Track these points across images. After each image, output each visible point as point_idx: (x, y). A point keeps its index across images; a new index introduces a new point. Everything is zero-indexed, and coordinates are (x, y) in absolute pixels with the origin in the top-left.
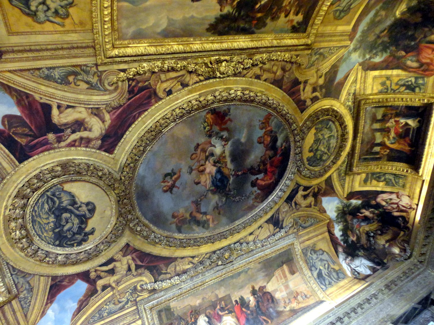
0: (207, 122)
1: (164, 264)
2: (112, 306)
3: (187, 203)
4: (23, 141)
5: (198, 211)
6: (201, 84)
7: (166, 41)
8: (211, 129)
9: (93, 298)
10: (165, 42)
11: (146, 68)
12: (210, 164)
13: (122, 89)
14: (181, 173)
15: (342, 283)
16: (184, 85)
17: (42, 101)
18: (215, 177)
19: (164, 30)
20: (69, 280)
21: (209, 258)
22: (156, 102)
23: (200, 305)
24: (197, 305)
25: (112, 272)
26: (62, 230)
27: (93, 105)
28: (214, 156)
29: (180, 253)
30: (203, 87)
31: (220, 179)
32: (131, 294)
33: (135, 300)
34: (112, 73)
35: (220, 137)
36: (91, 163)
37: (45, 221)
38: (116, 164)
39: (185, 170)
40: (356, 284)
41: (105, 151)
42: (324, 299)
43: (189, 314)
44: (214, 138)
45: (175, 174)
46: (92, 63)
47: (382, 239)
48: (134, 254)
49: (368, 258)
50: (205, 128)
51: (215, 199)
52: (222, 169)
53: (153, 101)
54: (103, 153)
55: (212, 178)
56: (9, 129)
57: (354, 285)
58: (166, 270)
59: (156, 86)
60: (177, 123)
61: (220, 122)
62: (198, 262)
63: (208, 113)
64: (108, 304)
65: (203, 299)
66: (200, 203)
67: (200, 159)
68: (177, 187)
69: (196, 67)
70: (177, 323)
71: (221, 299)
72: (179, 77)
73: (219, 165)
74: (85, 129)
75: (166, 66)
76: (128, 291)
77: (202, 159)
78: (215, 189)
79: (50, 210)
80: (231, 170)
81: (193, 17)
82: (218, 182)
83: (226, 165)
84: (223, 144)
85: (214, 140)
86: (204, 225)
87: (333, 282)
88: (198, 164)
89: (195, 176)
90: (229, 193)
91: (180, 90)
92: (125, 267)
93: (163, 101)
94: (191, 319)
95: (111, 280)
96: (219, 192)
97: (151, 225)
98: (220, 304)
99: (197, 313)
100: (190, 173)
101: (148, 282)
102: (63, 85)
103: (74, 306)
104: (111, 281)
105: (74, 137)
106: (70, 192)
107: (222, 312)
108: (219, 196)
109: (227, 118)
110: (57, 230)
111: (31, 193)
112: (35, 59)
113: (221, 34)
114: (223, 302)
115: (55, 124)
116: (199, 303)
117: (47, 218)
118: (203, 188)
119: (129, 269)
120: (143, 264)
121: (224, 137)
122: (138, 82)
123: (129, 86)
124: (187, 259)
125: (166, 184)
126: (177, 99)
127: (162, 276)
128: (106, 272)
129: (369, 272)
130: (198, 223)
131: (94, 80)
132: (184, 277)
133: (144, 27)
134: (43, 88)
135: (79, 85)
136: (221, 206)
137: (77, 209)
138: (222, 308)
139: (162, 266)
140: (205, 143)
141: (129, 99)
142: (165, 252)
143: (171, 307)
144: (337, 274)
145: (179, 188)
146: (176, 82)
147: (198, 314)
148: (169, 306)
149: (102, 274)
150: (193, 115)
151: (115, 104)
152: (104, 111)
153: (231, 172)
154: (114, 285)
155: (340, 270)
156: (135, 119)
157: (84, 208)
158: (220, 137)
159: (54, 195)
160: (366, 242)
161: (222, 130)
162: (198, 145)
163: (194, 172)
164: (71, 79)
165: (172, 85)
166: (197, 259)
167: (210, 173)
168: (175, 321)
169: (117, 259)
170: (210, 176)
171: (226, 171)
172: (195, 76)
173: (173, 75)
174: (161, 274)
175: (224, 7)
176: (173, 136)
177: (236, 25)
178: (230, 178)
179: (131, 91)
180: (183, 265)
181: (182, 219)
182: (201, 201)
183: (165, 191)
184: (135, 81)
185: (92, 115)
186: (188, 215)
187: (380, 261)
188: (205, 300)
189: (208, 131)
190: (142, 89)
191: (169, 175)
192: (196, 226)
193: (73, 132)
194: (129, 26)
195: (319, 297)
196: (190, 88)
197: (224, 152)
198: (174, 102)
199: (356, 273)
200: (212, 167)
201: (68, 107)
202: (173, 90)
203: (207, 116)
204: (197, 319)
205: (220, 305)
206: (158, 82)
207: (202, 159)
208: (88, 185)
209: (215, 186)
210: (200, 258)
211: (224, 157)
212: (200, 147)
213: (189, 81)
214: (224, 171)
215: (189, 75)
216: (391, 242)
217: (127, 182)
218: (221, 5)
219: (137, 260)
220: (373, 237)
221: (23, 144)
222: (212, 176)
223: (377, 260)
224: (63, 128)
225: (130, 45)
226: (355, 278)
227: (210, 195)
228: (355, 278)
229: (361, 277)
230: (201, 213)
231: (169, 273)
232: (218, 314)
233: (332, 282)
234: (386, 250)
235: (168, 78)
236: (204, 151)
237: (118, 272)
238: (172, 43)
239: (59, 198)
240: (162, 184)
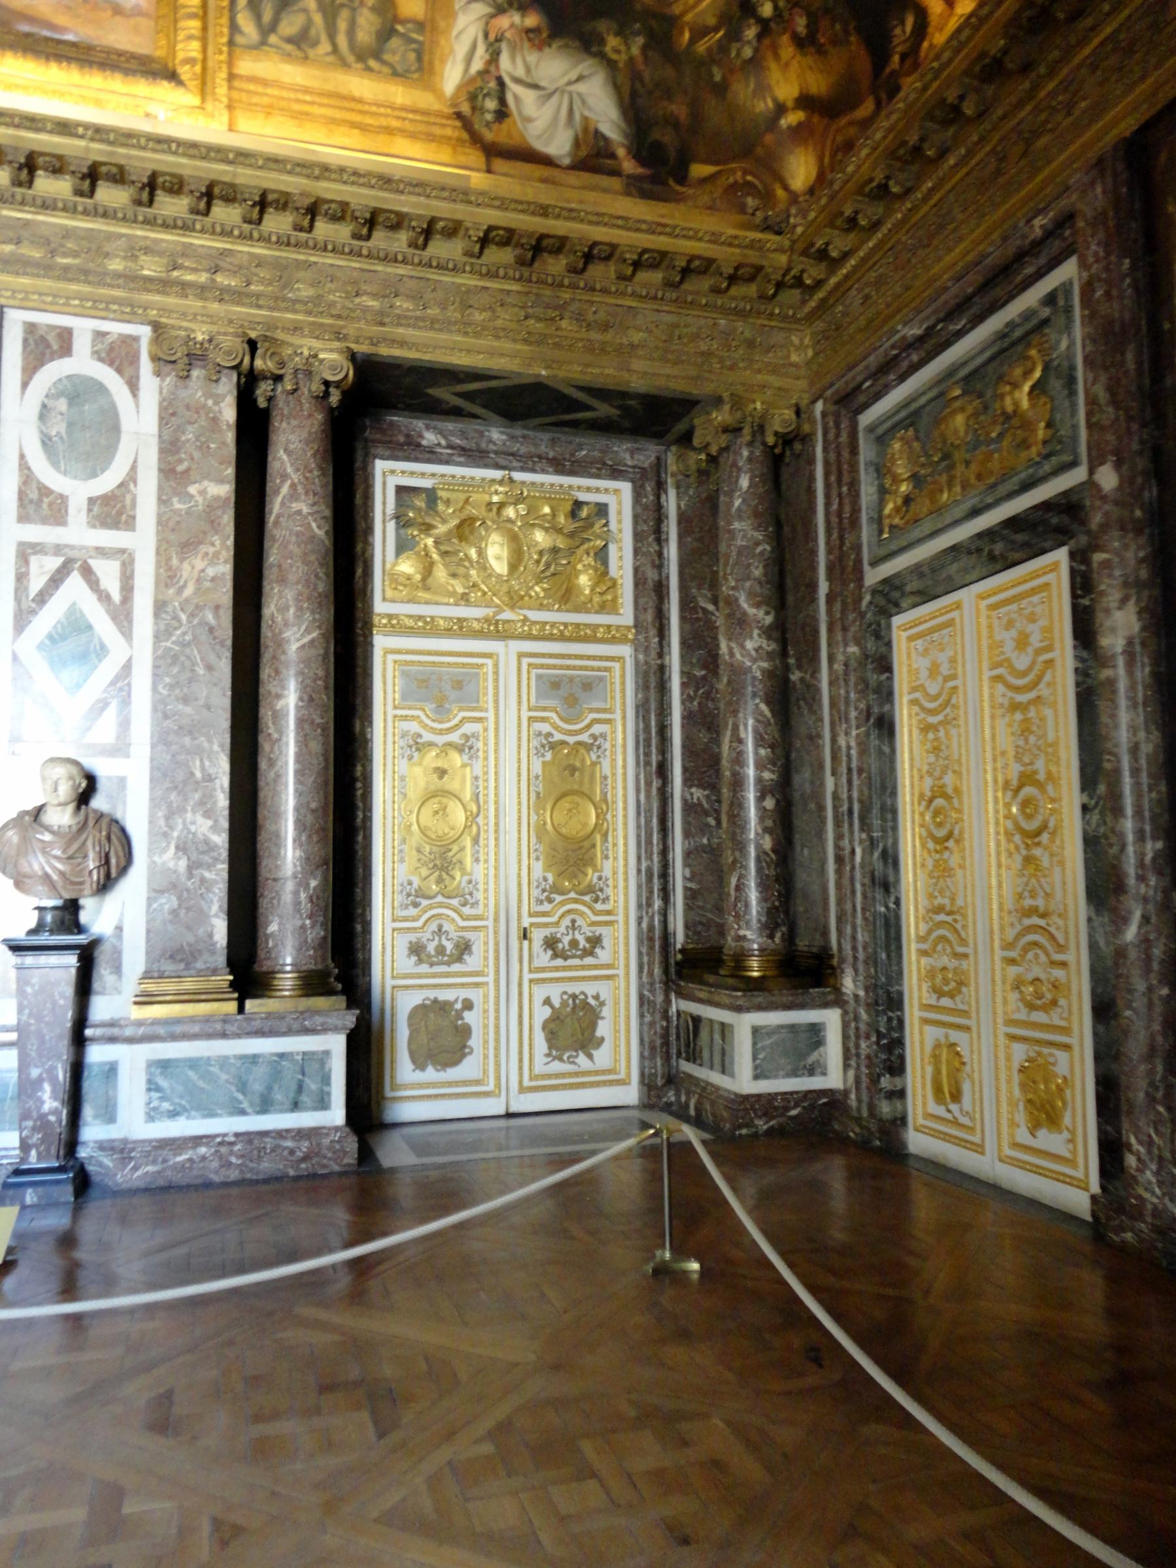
15: (361, 85)
40: (431, 138)
42: (184, 72)
47: (793, 72)
49: (634, 94)
57: (413, 136)
87: (325, 47)
129: (559, 146)
144: (386, 33)
155: (420, 26)
160: (712, 21)
187: (672, 154)
195: (173, 52)
199: (491, 104)
216: (816, 119)
220: (765, 28)
223: (666, 137)
226: (459, 116)
228: (459, 116)
229: (489, 136)
233: (315, 43)
234: (769, 138)
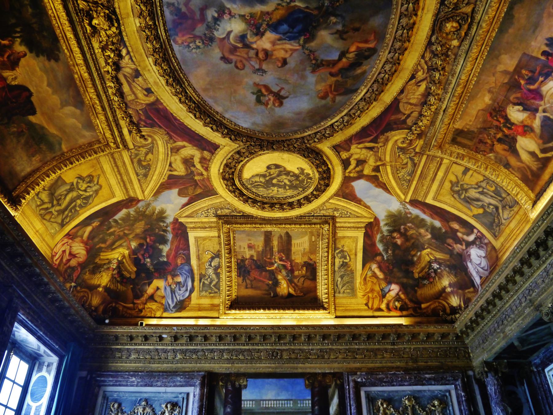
0: (189, 43)
1: (392, 115)
2: (404, 171)
3: (312, 79)
4: (199, 191)
5: (334, 63)
6: (132, 54)
7: (87, 102)
8: (200, 37)
9: (380, 179)
10: (89, 103)
11: (123, 115)
12: (258, 42)
13: (150, 132)
14: (262, 83)
16: (137, 74)
17: (166, 178)
18: (284, 34)
19: (76, 106)
20: (346, 188)
21: (435, 55)
22: (162, 104)
23: (494, 100)
24: (490, 102)
25: (361, 162)
26: (288, 185)
27: (168, 151)
28: (247, 34)
29: (388, 97)
30: (137, 52)
31: (289, 26)
32: (404, 153)
33: (416, 153)
34: (133, 139)
35: (215, 23)
36: (225, 162)
37: (275, 192)
38: (230, 145)
39: (257, 78)
41: (216, 150)
43: (490, 119)
44: (215, 33)
45: (260, 91)
46: (127, 152)
48: (353, 141)
50: (198, 47)
51: (325, 37)
52: (274, 20)
53: (160, 107)
54: (216, 152)
55: (285, 39)
56: (189, 195)
58: (405, 114)
59: (143, 104)
60: (189, 84)
61: (190, 22)
62: (428, 72)
63: (176, 42)
64: (398, 172)
65: (489, 91)
66: (319, 62)
67: (246, 56)
68: (280, 91)
69: (111, 64)
70: (485, 135)
71: (518, 70)
72: (128, 81)
73: (264, 26)
74: (193, 159)
75: (116, 99)
76: (399, 155)
77: (247, 54)
78: (305, 35)
79: (265, 188)
80: (279, 4)
81: (49, 85)
82: (295, 30)
83: (268, 13)
84: (229, 16)
85: (219, 34)
86: (365, 56)
88: (254, 60)
89: (271, 66)
90: (325, 8)
91: (145, 80)
92: (364, 151)
93: (159, 97)
94: (498, 120)
95: (372, 162)
96: (315, 28)
97: (322, 124)
98: (521, 76)
99: (499, 111)
100: (264, 72)
101: (404, 136)
102: (151, 168)
103: (379, 191)
104: (374, 164)
105: (198, 166)
106: (253, 176)
107: (534, 85)
108: (321, 29)
109: (184, 9)
110: (287, 188)
111: (244, 197)
112: (131, 182)
113: (55, 40)
114: (524, 72)
115: (186, 175)
116: (490, 100)
117: (273, 191)
118: (295, 55)
119: (371, 149)
120: (375, 135)
121: (216, 15)
122: (140, 119)
123: (145, 126)
124: (409, 87)
125: (271, 103)
126: (155, 83)
127: (409, 122)
128: (357, 165)
130: (356, 64)
131: (143, 150)
132: (432, 100)
133: (80, 125)
134: (154, 178)
135: (150, 159)
136: (344, 26)
137: (270, 175)
138: (529, 79)
139: (393, 117)
140: (222, 49)
141: (160, 127)
142: (375, 111)
143: (460, 128)
145: (282, 88)
146: (134, 84)
147: (501, 111)
148: (457, 130)
149: (357, 169)
150: (177, 65)
151: (166, 137)
152: (174, 145)
153: (284, 4)
154: (379, 163)
156: (182, 124)
157: (272, 171)
158: (215, 23)
159: (251, 184)
161: (203, 18)
162: (224, 59)
163: (264, 67)
164: (144, 163)
165: (139, 88)
166: (420, 73)
167: (274, 43)
168: (481, 136)
169: (348, 157)
170: (279, 42)
171: (277, 16)
172: (123, 60)
173: (126, 88)
174: (404, 122)
175: (19, 53)
176: (205, 90)
177: (34, 20)
178: (296, 6)
179: (152, 126)
180: (415, 93)
181: (335, 86)
182: (317, 60)
183: (281, 104)
184: (140, 122)
185: (178, 153)
186: (334, 79)
188: (494, 90)
189: (203, 43)
190: (148, 117)
191: (260, 97)
192: (358, 68)
193: (194, 166)
194: (84, 136)
196: (139, 69)
197: (242, 17)
198: (160, 87)
200: (264, 38)
201: (170, 165)
202: (145, 87)
203: (180, 42)
204: (506, 116)
205: (523, 78)
206: (138, 102)
207: (247, 54)
208: (248, 164)
209: (301, 36)
210: (423, 68)
211: (252, 15)
212: (227, 55)
213: (132, 69)
214: (278, 17)
215: (124, 69)
217: (252, 143)
218: (19, 59)
219: (364, 140)
221: (202, 191)
222: (279, 40)
224: (190, 171)
225: (102, 133)
227: (313, 45)
230: (340, 59)
231: (412, 113)
232: (530, 91)
235: (130, 93)
236: (234, 50)
237: (366, 158)
238: (88, 97)
239: (256, 182)
240: (269, 106)
